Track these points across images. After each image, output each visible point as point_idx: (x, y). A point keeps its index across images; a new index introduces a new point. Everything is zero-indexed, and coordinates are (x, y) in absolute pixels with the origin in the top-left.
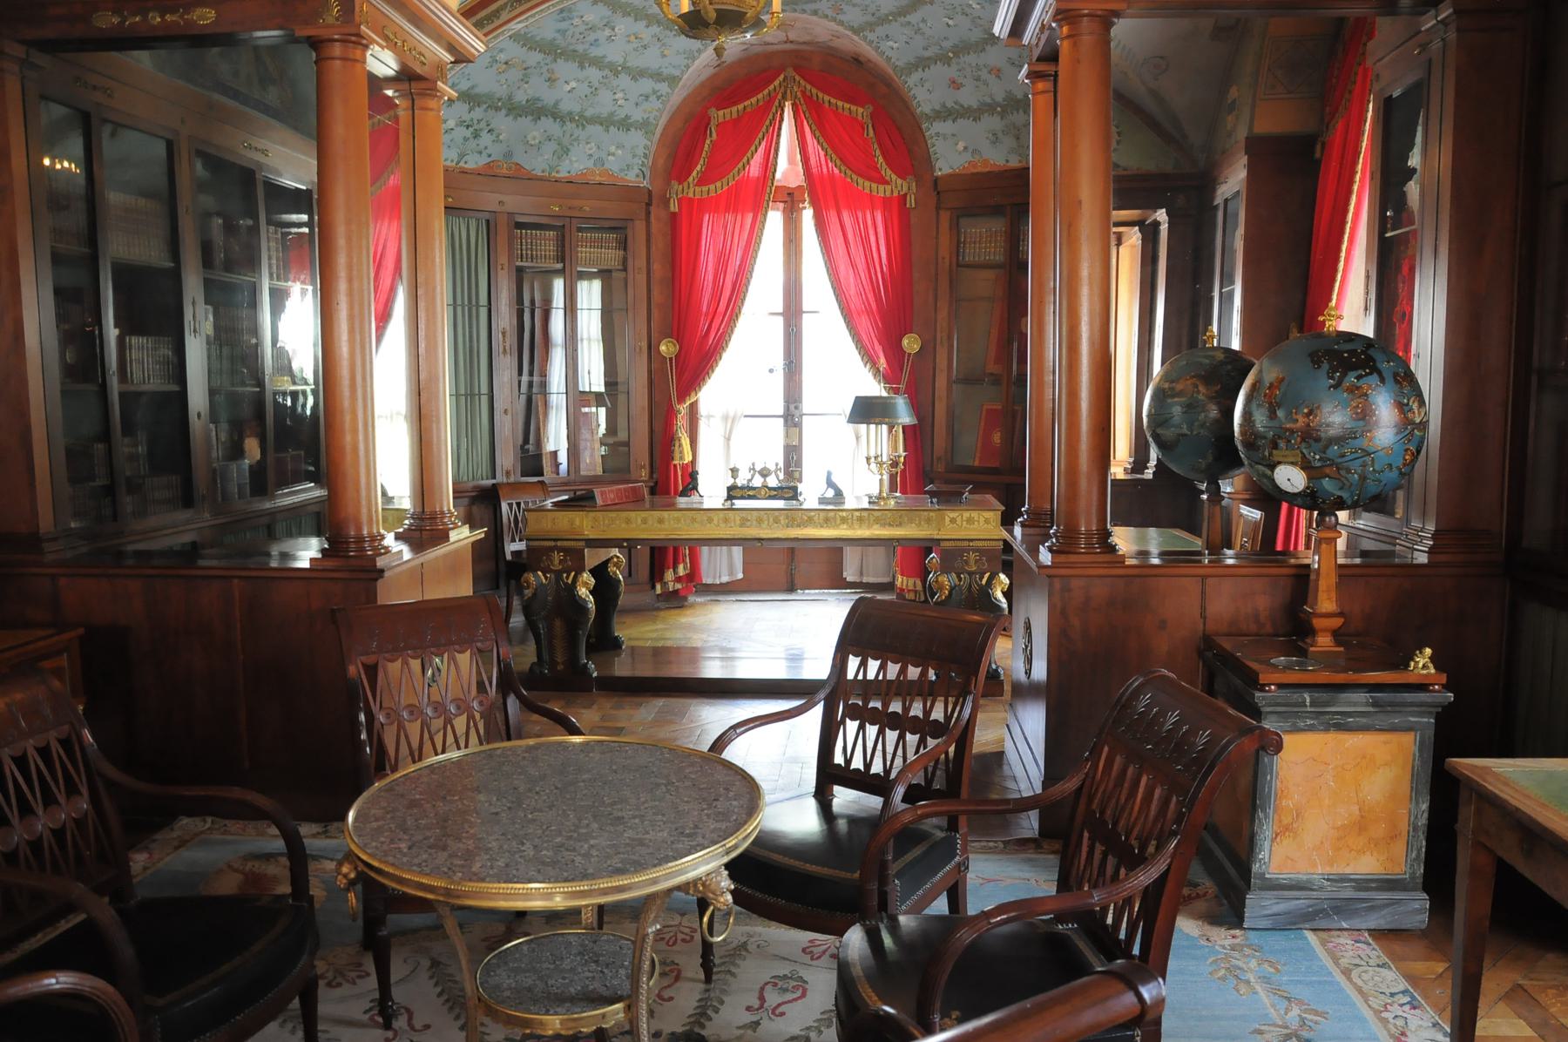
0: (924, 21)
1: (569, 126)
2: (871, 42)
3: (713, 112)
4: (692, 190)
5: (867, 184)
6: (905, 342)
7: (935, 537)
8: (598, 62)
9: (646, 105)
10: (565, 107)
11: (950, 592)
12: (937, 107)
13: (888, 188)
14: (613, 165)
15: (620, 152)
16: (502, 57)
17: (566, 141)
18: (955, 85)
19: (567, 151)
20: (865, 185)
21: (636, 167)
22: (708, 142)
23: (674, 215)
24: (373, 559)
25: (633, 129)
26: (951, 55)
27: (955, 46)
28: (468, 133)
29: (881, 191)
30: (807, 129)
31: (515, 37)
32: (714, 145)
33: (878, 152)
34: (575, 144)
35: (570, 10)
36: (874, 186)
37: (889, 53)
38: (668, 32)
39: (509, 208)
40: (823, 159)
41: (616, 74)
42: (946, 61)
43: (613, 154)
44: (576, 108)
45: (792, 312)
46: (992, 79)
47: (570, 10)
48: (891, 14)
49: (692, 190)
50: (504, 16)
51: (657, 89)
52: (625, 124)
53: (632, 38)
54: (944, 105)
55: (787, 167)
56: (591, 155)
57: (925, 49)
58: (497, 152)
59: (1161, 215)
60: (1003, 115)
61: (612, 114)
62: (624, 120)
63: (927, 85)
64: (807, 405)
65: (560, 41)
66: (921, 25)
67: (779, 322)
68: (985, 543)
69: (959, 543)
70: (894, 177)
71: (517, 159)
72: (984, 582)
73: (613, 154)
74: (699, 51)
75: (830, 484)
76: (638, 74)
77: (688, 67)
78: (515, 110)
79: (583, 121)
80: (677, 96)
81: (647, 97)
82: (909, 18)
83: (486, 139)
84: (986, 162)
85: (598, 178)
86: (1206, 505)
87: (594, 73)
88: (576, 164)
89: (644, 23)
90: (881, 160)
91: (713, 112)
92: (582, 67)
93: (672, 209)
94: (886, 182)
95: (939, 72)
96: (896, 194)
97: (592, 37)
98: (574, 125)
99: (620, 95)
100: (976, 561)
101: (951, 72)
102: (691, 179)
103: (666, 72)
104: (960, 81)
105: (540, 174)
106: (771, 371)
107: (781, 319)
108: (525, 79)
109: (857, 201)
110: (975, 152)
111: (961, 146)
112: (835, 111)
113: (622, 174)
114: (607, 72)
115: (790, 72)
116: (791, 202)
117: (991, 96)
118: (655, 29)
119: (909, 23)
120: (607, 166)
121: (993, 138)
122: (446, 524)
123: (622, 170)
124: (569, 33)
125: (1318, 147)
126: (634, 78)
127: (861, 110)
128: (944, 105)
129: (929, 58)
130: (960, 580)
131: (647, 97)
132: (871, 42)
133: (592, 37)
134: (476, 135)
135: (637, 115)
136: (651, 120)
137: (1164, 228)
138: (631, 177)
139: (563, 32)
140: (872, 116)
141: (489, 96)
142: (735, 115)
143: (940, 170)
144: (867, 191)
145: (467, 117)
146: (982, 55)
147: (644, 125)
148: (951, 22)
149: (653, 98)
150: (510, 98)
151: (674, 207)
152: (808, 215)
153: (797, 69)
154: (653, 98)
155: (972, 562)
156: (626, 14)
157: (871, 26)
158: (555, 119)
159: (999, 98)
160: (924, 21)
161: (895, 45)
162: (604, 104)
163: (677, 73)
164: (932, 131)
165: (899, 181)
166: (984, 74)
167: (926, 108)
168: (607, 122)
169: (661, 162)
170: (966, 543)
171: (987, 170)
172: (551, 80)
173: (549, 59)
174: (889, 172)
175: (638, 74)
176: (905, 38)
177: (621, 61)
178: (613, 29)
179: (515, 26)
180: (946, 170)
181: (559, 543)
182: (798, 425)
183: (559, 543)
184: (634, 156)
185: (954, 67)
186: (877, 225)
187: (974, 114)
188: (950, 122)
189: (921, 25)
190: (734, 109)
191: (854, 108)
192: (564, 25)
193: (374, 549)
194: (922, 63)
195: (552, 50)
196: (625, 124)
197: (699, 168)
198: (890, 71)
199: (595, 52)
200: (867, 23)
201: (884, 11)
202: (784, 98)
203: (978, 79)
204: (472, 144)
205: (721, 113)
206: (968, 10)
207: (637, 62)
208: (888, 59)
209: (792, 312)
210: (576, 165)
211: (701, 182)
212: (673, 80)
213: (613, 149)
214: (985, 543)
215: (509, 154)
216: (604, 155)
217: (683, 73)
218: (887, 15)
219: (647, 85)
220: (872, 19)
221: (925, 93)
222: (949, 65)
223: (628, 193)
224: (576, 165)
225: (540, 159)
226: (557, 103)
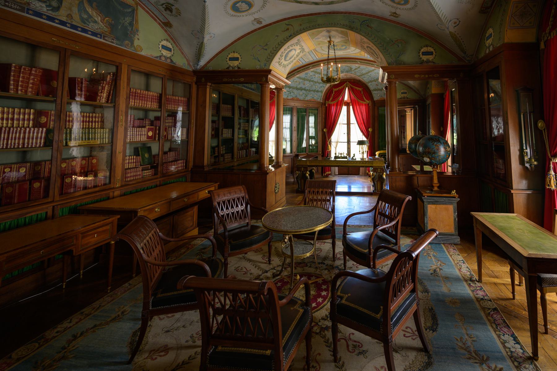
1: (307, 92)
3: (334, 89)
4: (330, 103)
8: (313, 81)
10: (307, 88)
14: (315, 98)
16: (295, 80)
20: (361, 102)
23: (326, 107)
24: (267, 171)
28: (289, 93)
29: (364, 103)
31: (298, 77)
32: (334, 95)
39: (296, 105)
41: (316, 83)
44: (309, 89)
50: (296, 74)
52: (318, 91)
55: (346, 98)
58: (294, 96)
61: (315, 90)
71: (298, 97)
78: (297, 89)
79: (310, 91)
81: (321, 87)
83: (292, 94)
87: (312, 83)
88: (308, 98)
91: (334, 89)
92: (310, 82)
108: (299, 84)
109: (359, 104)
111: (379, 95)
112: (356, 90)
115: (348, 82)
116: (347, 104)
131: (321, 87)
134: (290, 93)
135: (320, 90)
138: (319, 100)
139: (306, 77)
141: (293, 87)
145: (289, 90)
147: (321, 92)
149: (323, 87)
150: (297, 87)
151: (327, 105)
152: (351, 107)
153: (349, 82)
168: (314, 91)
169: (324, 97)
172: (304, 84)
179: (298, 76)
186: (364, 109)
193: (267, 169)
195: (304, 79)
199: (312, 80)
202: (346, 87)
204: (290, 95)
211: (332, 101)
215: (296, 96)
216: (313, 96)
223: (318, 103)
226: (305, 88)
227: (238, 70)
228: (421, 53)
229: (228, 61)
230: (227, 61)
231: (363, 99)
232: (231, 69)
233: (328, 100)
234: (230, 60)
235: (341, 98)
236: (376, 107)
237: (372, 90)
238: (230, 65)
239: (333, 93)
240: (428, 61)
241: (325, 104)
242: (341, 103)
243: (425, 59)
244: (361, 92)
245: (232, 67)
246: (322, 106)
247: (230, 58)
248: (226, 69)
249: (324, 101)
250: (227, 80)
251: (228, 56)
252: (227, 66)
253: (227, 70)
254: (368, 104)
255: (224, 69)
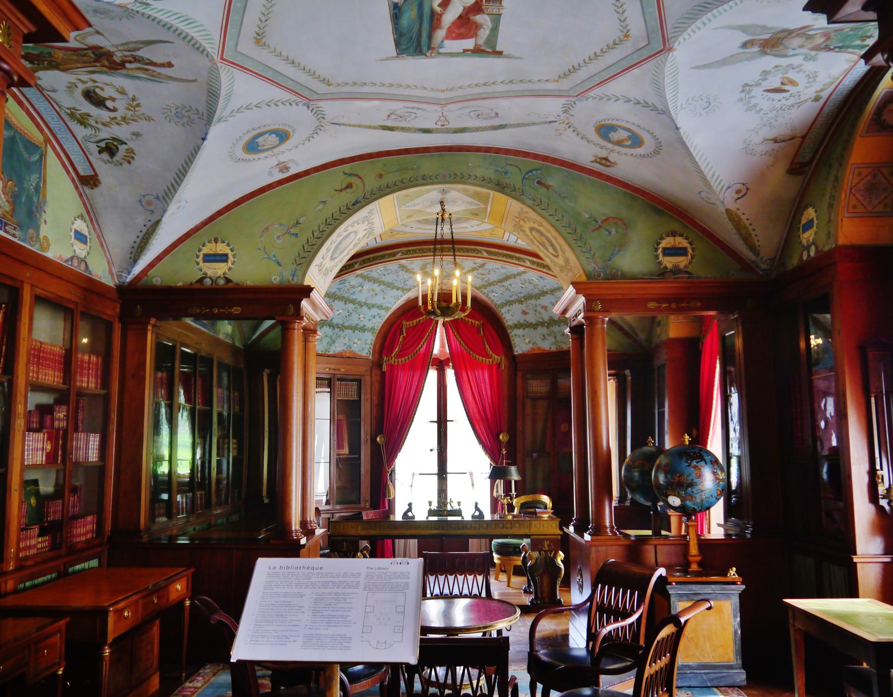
0: (510, 285)
1: (337, 330)
2: (484, 293)
3: (404, 323)
4: (393, 361)
5: (480, 358)
6: (501, 437)
7: (529, 534)
8: (353, 302)
9: (374, 320)
10: (335, 322)
11: (536, 560)
12: (516, 323)
13: (491, 360)
14: (356, 349)
15: (359, 342)
17: (334, 337)
18: (525, 313)
19: (334, 342)
21: (366, 350)
22: (401, 337)
23: (384, 373)
25: (366, 331)
26: (523, 300)
27: (525, 296)
30: (451, 331)
32: (404, 338)
33: (486, 343)
34: (338, 338)
35: (345, 280)
36: (484, 359)
37: (493, 298)
38: (388, 288)
40: (459, 345)
41: (361, 306)
42: (520, 302)
43: (356, 343)
44: (340, 322)
45: (442, 421)
46: (543, 311)
47: (345, 280)
48: (495, 281)
49: (393, 360)
51: (379, 313)
52: (363, 329)
53: (371, 291)
54: (519, 322)
56: (345, 344)
57: (511, 297)
59: (627, 372)
60: (548, 327)
61: (357, 324)
62: (363, 327)
63: (510, 312)
64: (450, 468)
65: (338, 293)
66: (509, 287)
67: (435, 426)
68: (552, 537)
69: (540, 537)
70: (493, 355)
72: (552, 555)
73: (356, 343)
74: (401, 296)
75: (477, 509)
76: (370, 307)
77: (395, 303)
79: (343, 328)
80: (386, 315)
81: (375, 316)
82: (503, 284)
84: (539, 349)
85: (348, 355)
86: (653, 517)
87: (350, 306)
89: (377, 284)
90: (487, 346)
91: (404, 323)
92: (346, 303)
93: (384, 370)
94: (491, 358)
95: (517, 307)
96: (495, 363)
97: (352, 291)
98: (339, 330)
99: (362, 316)
100: (548, 546)
101: (523, 307)
102: (393, 355)
103: (384, 306)
104: (527, 311)
105: (320, 353)
106: (431, 450)
107: (436, 425)
109: (475, 366)
110: (534, 343)
111: (527, 341)
113: (359, 353)
114: (357, 305)
116: (441, 366)
117: (542, 318)
118: (382, 287)
119: (503, 286)
120: (352, 349)
121: (543, 338)
122: (311, 527)
123: (360, 351)
124: (343, 289)
125: (700, 344)
126: (369, 308)
127: (477, 322)
128: (519, 322)
129: (512, 301)
130: (540, 554)
132: (484, 293)
133: (352, 291)
135: (369, 325)
136: (376, 327)
137: (629, 378)
138: (364, 354)
139: (339, 289)
140: (483, 325)
142: (415, 324)
143: (517, 351)
144: (481, 361)
146: (538, 300)
147: (373, 329)
148: (523, 286)
149: (377, 317)
151: (384, 368)
152: (450, 373)
154: (377, 317)
155: (546, 546)
156: (370, 281)
157: (485, 287)
158: (330, 327)
159: (546, 319)
160: (510, 285)
161: (496, 295)
162: (354, 320)
163: (389, 306)
164: (513, 334)
165: (496, 357)
166: (539, 309)
167: (510, 323)
168: (354, 328)
169: (377, 346)
170: (543, 537)
171: (540, 352)
173: (331, 300)
174: (491, 352)
175: (370, 307)
176: (500, 292)
177: (364, 301)
178: (363, 287)
180: (520, 352)
181: (346, 538)
182: (446, 479)
183: (346, 538)
184: (366, 344)
185: (524, 305)
187: (534, 326)
188: (522, 330)
189: (509, 287)
190: (415, 321)
191: (473, 321)
192: (342, 286)
194: (509, 303)
196: (363, 329)
197: (397, 350)
198: (493, 306)
199: (353, 297)
200: (483, 285)
201: (491, 280)
203: (536, 311)
205: (408, 323)
206: (532, 282)
207: (371, 301)
208: (493, 301)
209: (442, 421)
210: (338, 348)
211: (398, 356)
212: (387, 309)
213: (356, 341)
214: (552, 537)
216: (351, 343)
217: (393, 306)
218: (493, 282)
219: (375, 311)
220: (485, 283)
221: (510, 316)
222: (522, 304)
224: (338, 348)
225: (321, 346)
227: (226, 286)
228: (660, 250)
229: (201, 264)
230: (198, 264)
231: (485, 349)
232: (208, 282)
233: (389, 354)
234: (205, 261)
235: (425, 346)
236: (519, 374)
237: (511, 327)
238: (205, 274)
239: (401, 333)
240: (676, 270)
241: (380, 366)
242: (425, 361)
243: (669, 266)
244: (479, 330)
245: (211, 278)
246: (371, 371)
247: (205, 255)
248: (197, 282)
249: (377, 356)
250: (198, 311)
251: (200, 250)
252: (199, 275)
253: (198, 286)
254: (499, 364)
255: (191, 284)
